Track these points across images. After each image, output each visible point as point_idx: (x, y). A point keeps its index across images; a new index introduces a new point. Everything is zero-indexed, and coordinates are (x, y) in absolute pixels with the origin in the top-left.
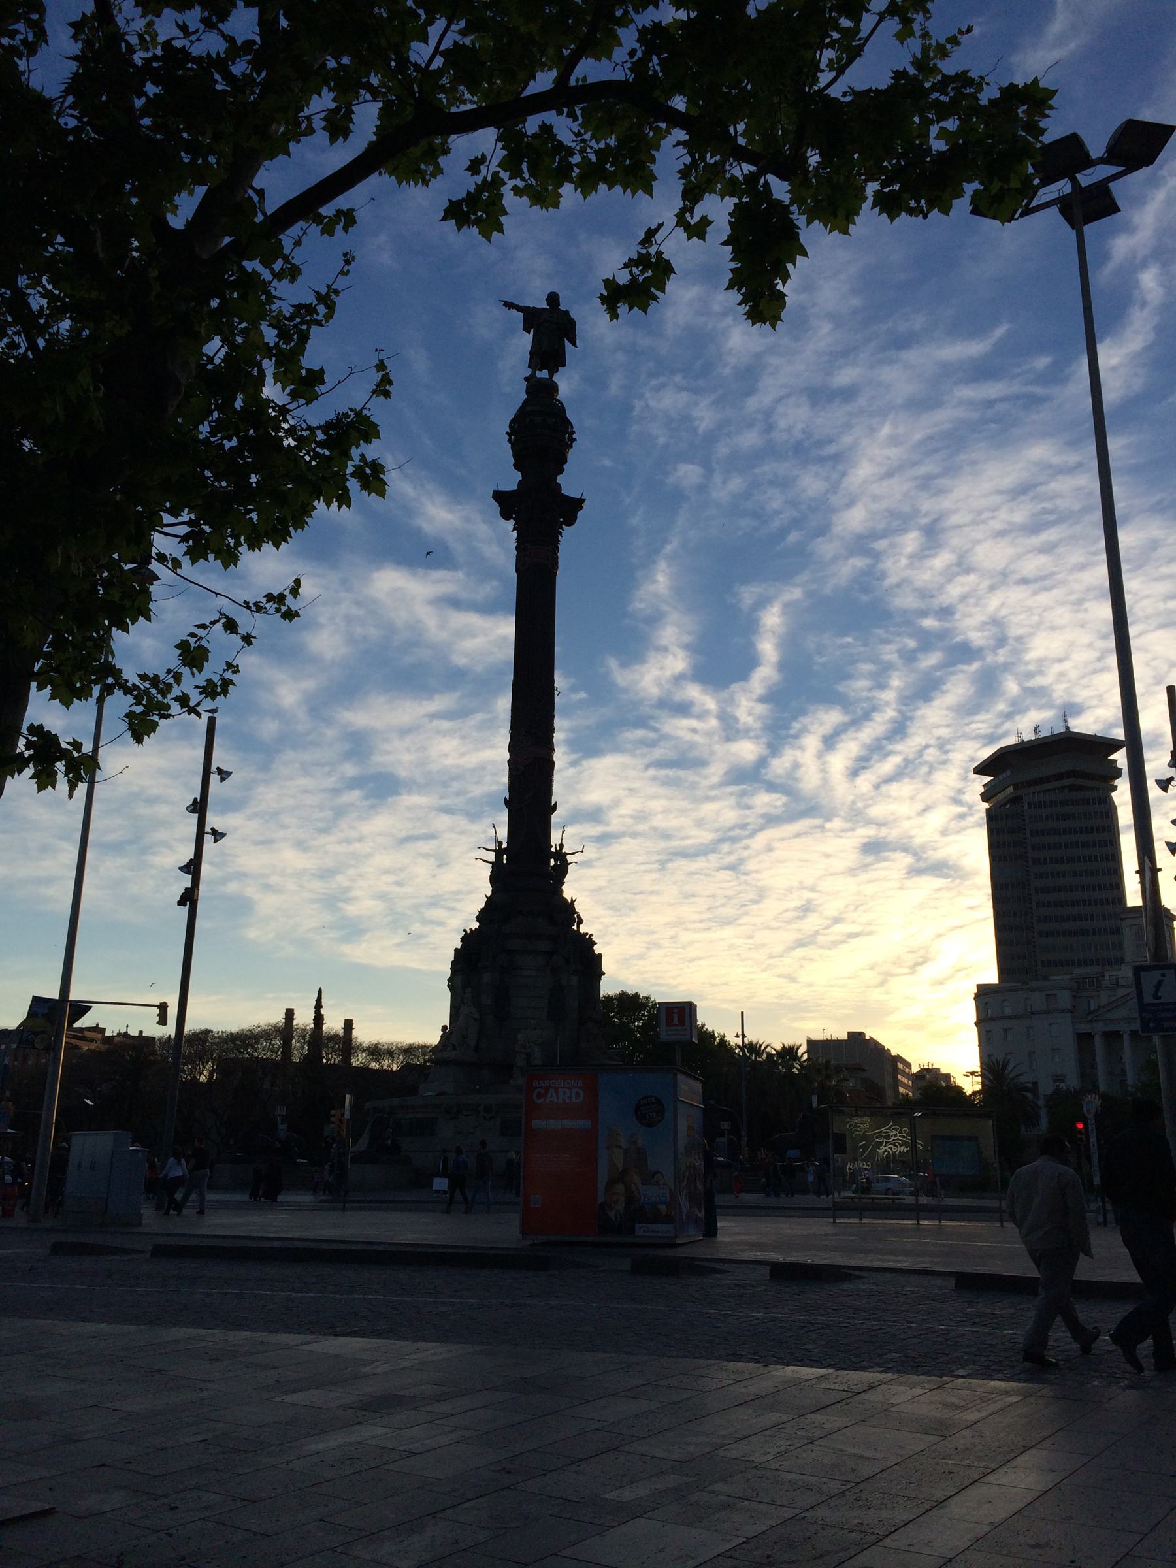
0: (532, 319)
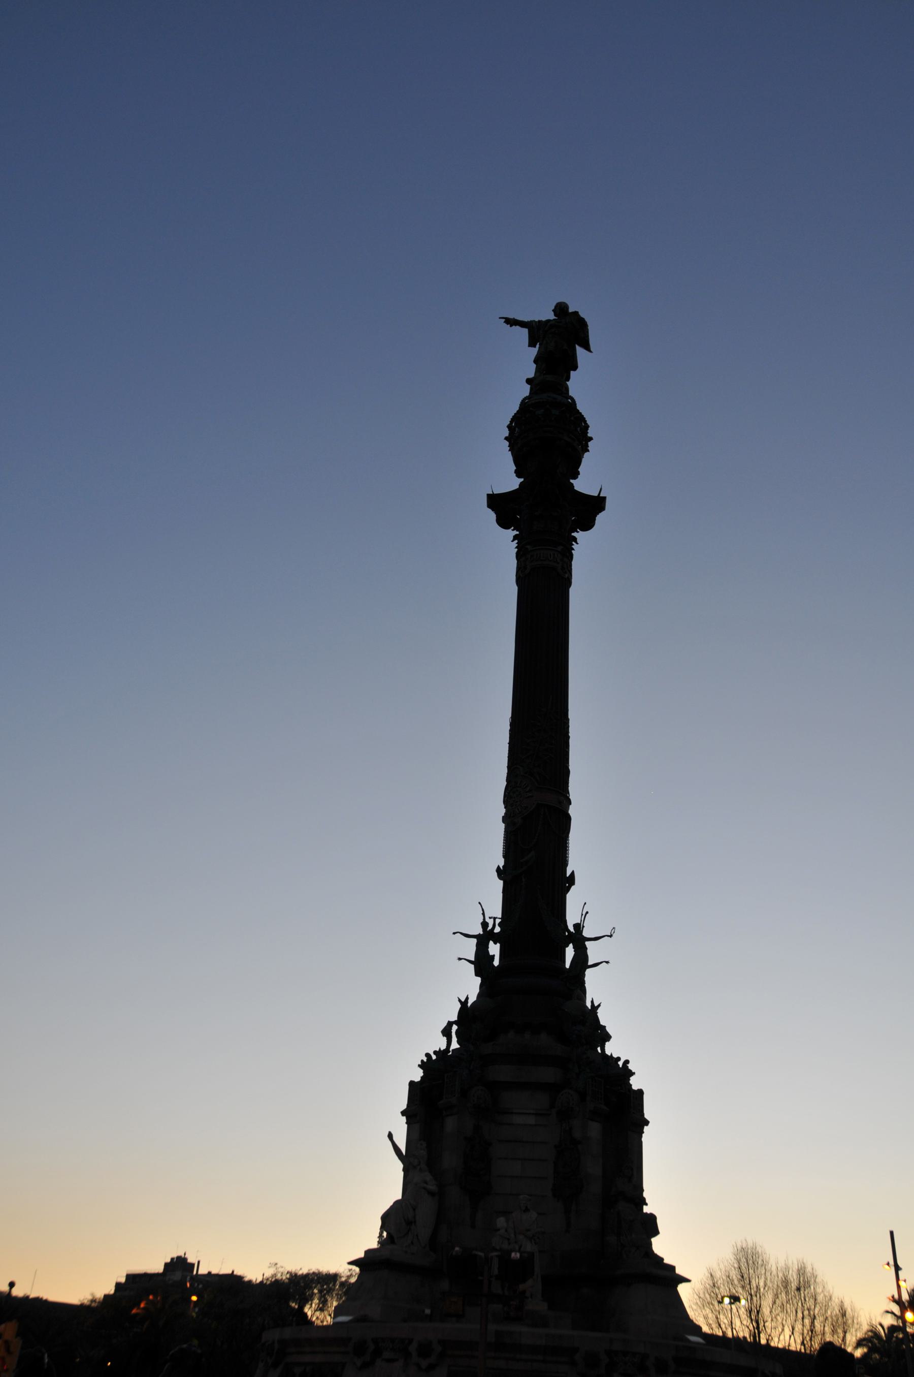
0: (537, 332)
